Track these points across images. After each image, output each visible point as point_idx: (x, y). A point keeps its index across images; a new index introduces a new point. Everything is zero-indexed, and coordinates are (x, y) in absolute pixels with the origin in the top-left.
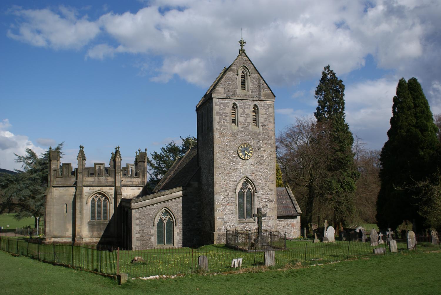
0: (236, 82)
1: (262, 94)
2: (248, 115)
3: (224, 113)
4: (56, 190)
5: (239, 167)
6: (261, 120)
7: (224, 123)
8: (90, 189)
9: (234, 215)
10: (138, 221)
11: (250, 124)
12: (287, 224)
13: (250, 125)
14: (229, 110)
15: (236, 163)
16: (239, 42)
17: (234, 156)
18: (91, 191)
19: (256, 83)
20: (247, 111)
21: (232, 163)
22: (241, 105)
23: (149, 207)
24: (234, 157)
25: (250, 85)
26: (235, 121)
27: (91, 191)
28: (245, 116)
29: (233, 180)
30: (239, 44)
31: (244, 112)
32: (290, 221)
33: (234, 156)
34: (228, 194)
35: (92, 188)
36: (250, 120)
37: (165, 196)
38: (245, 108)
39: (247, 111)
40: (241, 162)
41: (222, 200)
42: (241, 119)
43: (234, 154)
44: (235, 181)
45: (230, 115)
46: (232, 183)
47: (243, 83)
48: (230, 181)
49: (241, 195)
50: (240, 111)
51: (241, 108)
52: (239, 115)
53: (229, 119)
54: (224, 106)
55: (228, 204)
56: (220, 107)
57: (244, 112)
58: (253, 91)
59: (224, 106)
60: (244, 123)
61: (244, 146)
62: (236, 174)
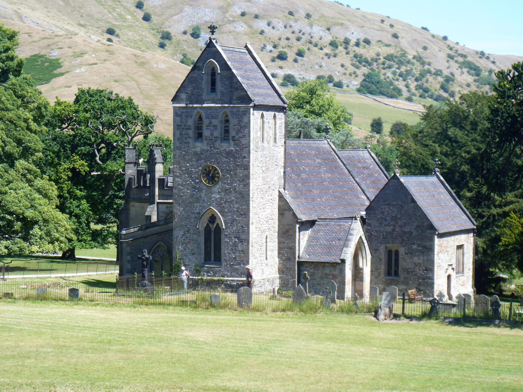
0: (202, 83)
1: (234, 98)
2: (215, 126)
3: (185, 125)
4: (133, 206)
5: (203, 196)
6: (232, 133)
7: (186, 138)
8: (167, 207)
9: (196, 256)
10: (129, 257)
11: (218, 139)
12: (326, 274)
13: (217, 140)
14: (191, 122)
15: (200, 190)
16: (209, 28)
17: (197, 181)
18: (168, 209)
19: (227, 82)
20: (215, 122)
21: (194, 191)
22: (208, 114)
23: (142, 240)
24: (197, 183)
25: (219, 86)
26: (199, 136)
27: (168, 209)
28: (212, 128)
29: (196, 212)
30: (209, 30)
31: (211, 123)
32: (330, 271)
33: (197, 181)
34: (189, 230)
35: (169, 205)
36: (216, 134)
37: (159, 227)
38: (213, 118)
39: (215, 122)
40: (205, 189)
41: (182, 237)
42: (206, 133)
43: (197, 179)
44: (197, 213)
45: (193, 128)
46: (193, 216)
47: (213, 83)
48: (192, 213)
49: (207, 229)
50: (206, 122)
51: (207, 118)
52: (204, 127)
53: (191, 133)
54: (187, 117)
55: (189, 242)
56: (182, 118)
57: (211, 123)
58: (222, 94)
59: (187, 117)
60: (211, 138)
61: (209, 168)
62: (199, 204)
